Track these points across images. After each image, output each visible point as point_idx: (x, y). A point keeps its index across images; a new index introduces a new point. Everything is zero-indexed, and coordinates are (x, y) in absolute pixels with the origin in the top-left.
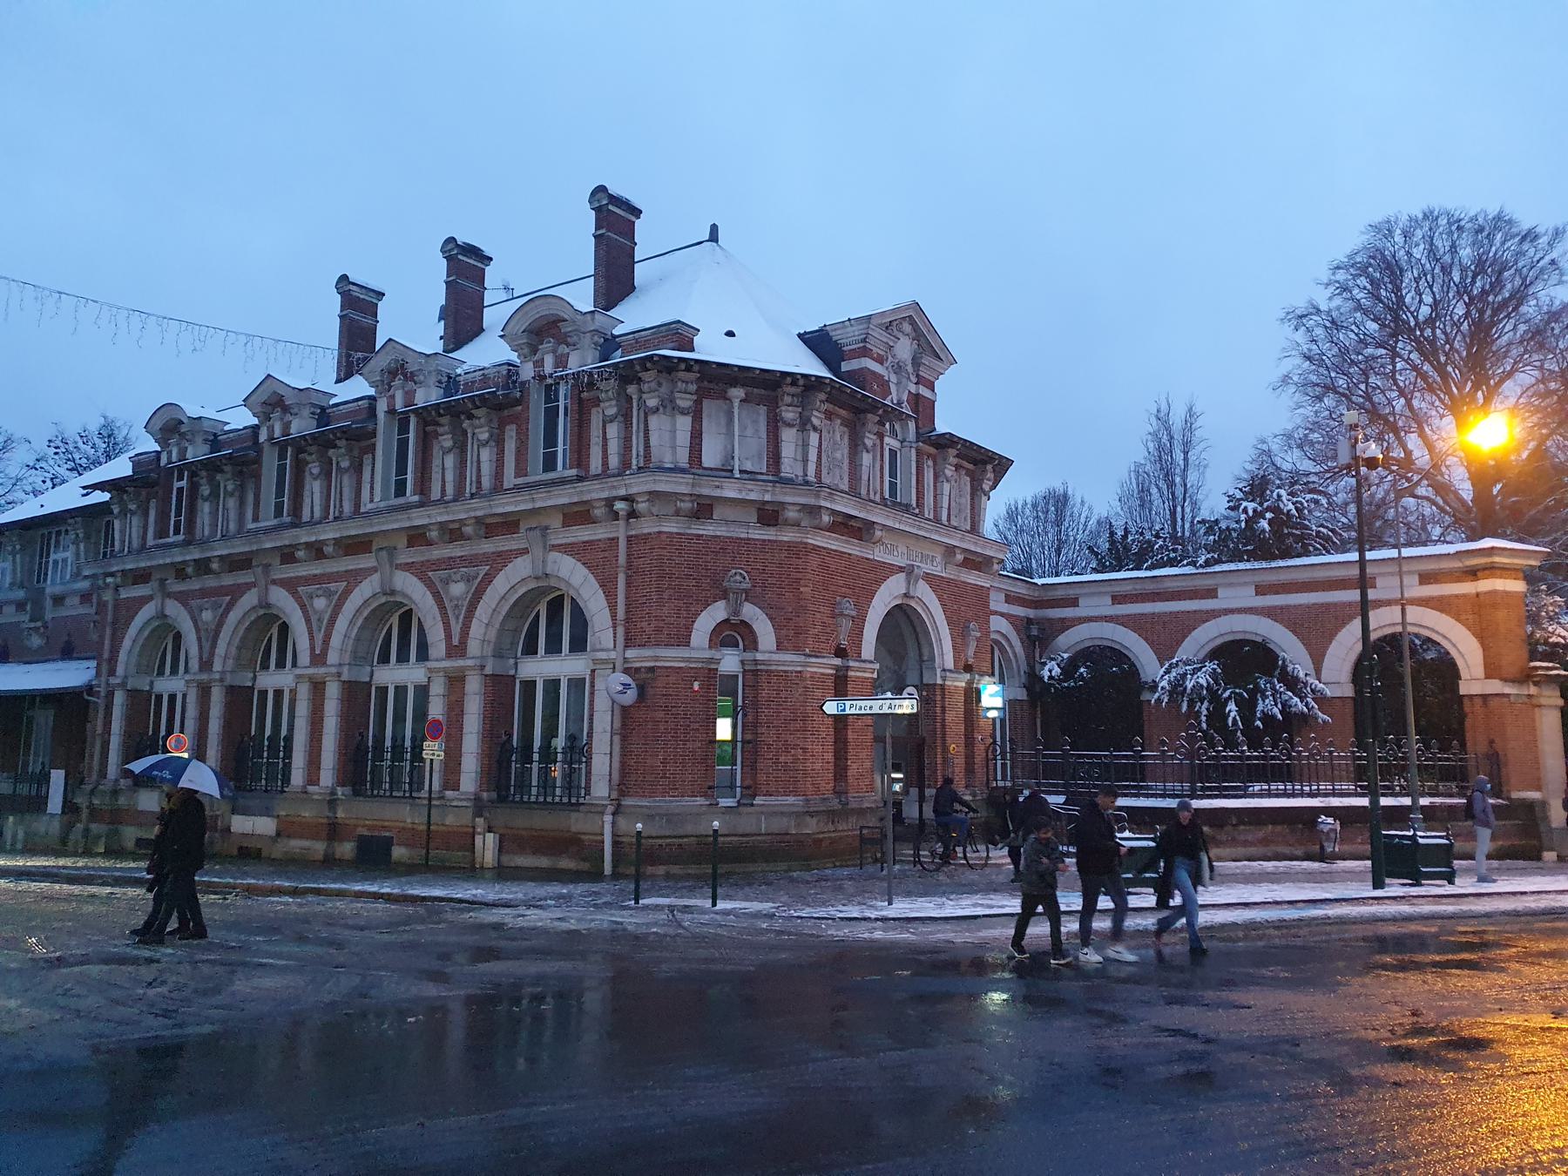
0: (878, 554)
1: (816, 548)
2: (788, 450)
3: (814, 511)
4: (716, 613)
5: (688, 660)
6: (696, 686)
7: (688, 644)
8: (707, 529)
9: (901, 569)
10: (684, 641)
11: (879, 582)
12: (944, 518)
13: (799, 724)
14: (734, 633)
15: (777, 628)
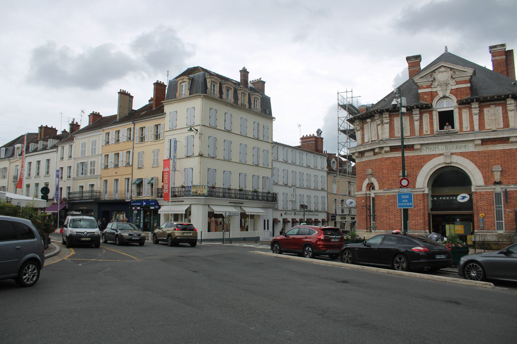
0: (425, 152)
1: (388, 158)
2: (380, 132)
3: (382, 148)
4: (366, 182)
5: (361, 194)
6: (363, 201)
7: (361, 190)
8: (364, 159)
9: (440, 155)
10: (361, 190)
11: (425, 162)
12: (476, 128)
13: (384, 210)
14: (371, 186)
15: (379, 183)
